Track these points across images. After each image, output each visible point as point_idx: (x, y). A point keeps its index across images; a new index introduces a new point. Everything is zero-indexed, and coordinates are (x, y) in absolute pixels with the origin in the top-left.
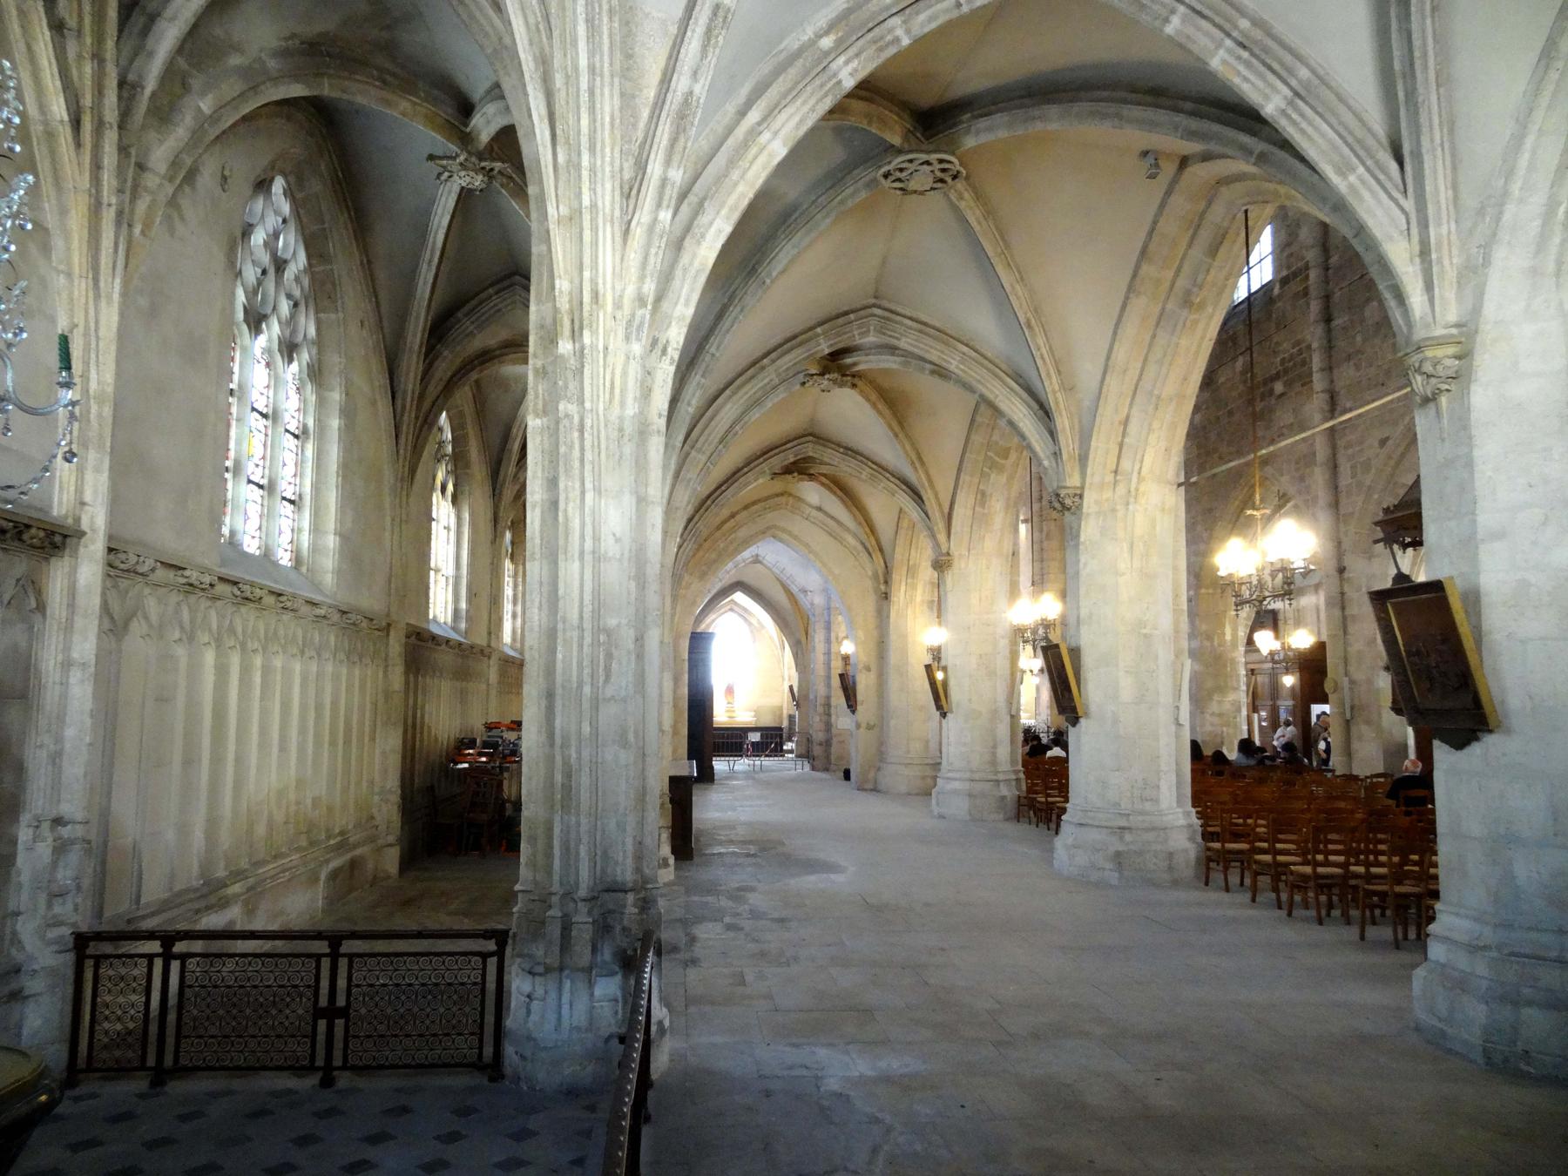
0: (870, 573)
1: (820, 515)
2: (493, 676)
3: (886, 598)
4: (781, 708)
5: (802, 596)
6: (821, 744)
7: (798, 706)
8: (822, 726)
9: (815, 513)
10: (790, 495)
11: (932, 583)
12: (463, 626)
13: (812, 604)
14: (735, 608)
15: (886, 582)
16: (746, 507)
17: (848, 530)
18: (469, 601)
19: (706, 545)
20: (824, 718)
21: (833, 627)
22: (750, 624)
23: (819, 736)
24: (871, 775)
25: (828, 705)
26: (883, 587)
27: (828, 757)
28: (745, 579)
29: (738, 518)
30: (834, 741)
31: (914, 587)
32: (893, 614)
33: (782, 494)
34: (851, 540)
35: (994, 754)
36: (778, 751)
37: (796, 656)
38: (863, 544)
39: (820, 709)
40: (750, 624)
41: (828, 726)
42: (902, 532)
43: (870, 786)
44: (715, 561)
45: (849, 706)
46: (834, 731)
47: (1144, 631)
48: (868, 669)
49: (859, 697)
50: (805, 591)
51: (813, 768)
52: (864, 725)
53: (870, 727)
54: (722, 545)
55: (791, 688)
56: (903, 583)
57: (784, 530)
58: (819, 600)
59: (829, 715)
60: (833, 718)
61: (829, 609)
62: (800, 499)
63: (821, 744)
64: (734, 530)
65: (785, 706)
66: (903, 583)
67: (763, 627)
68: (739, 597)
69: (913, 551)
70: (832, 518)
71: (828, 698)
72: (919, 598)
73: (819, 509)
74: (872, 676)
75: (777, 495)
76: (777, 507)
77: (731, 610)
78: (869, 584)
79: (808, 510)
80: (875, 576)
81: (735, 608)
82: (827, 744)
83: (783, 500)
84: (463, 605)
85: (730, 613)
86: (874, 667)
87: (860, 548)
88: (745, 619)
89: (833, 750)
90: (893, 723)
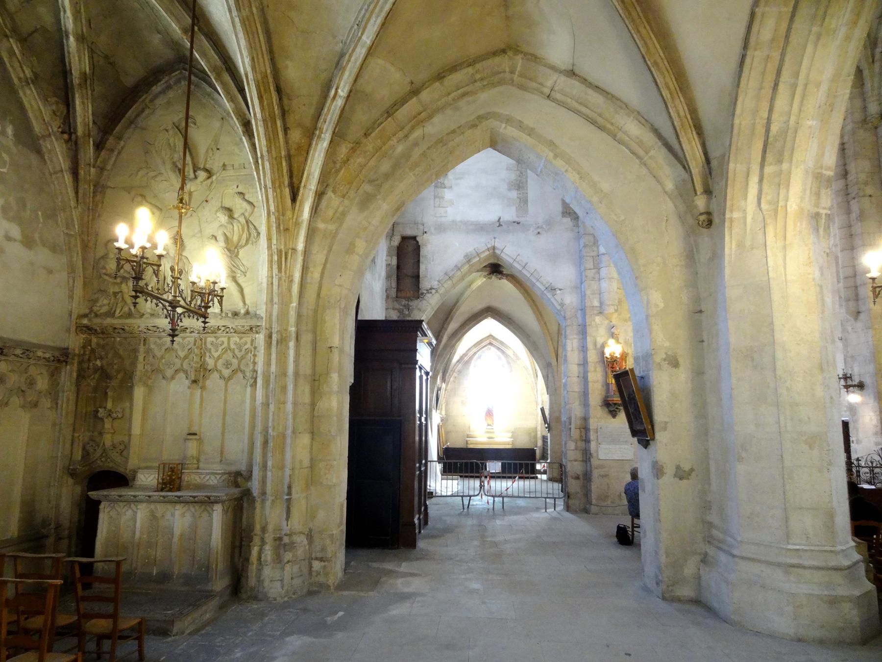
0: (670, 186)
1: (575, 87)
3: (710, 223)
4: (535, 430)
5: (549, 295)
6: (577, 478)
7: (549, 428)
8: (578, 455)
9: (563, 82)
10: (517, 50)
11: (818, 177)
13: (562, 305)
14: (494, 342)
15: (708, 192)
16: (439, 77)
17: (625, 106)
19: (370, 145)
20: (582, 445)
21: (589, 330)
22: (507, 356)
23: (574, 467)
24: (689, 570)
25: (585, 428)
26: (701, 202)
27: (587, 494)
28: (495, 304)
29: (425, 95)
30: (595, 474)
31: (782, 181)
32: (730, 247)
33: (504, 51)
34: (633, 128)
36: (530, 472)
37: (546, 378)
38: (656, 132)
39: (575, 434)
40: (507, 356)
41: (586, 456)
42: (756, 58)
43: (686, 592)
44: (387, 176)
45: (634, 433)
46: (594, 462)
48: (674, 363)
49: (659, 416)
50: (553, 290)
51: (568, 508)
52: (670, 470)
53: (681, 474)
54: (400, 149)
55: (542, 410)
56: (754, 180)
57: (509, 120)
58: (570, 299)
59: (587, 441)
60: (593, 445)
61: (583, 309)
62: (534, 58)
63: (577, 478)
64: (418, 121)
65: (539, 428)
66: (754, 180)
67: (518, 358)
68: (489, 326)
69: (781, 102)
70: (597, 88)
71: (585, 419)
72: (793, 205)
73: (572, 73)
74: (683, 376)
75: (495, 54)
76: (495, 80)
77: (490, 344)
78: (668, 207)
79: (552, 80)
80: (685, 192)
81: (494, 342)
82: (586, 477)
83: (503, 62)
85: (489, 346)
86: (685, 363)
87: (649, 138)
88: (503, 352)
89: (594, 486)
90: (741, 469)
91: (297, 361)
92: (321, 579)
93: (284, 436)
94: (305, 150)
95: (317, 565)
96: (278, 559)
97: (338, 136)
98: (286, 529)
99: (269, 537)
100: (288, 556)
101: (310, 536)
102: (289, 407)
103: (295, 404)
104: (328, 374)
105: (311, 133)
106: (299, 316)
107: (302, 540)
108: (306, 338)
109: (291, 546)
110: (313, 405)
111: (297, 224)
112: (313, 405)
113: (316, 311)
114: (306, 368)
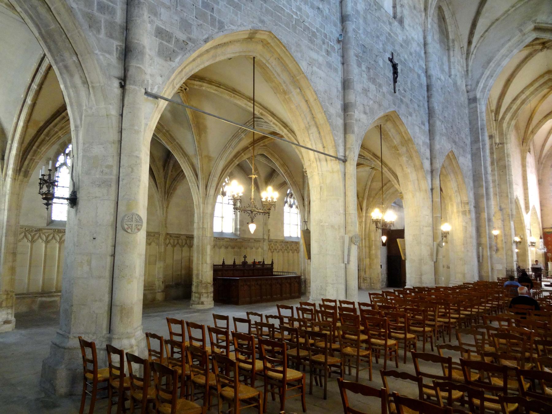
2: (266, 247)
12: (238, 233)
18: (240, 225)
35: (421, 278)
47: (321, 224)
84: (238, 227)
91: (365, 244)
92: (373, 287)
93: (363, 259)
94: (363, 201)
95: (372, 284)
96: (364, 282)
97: (369, 196)
98: (365, 276)
99: (362, 278)
100: (365, 282)
101: (370, 279)
102: (364, 253)
103: (365, 252)
104: (372, 246)
105: (363, 198)
106: (365, 235)
107: (368, 279)
108: (367, 239)
109: (366, 280)
110: (370, 252)
111: (363, 216)
112: (370, 252)
113: (369, 233)
114: (367, 244)
